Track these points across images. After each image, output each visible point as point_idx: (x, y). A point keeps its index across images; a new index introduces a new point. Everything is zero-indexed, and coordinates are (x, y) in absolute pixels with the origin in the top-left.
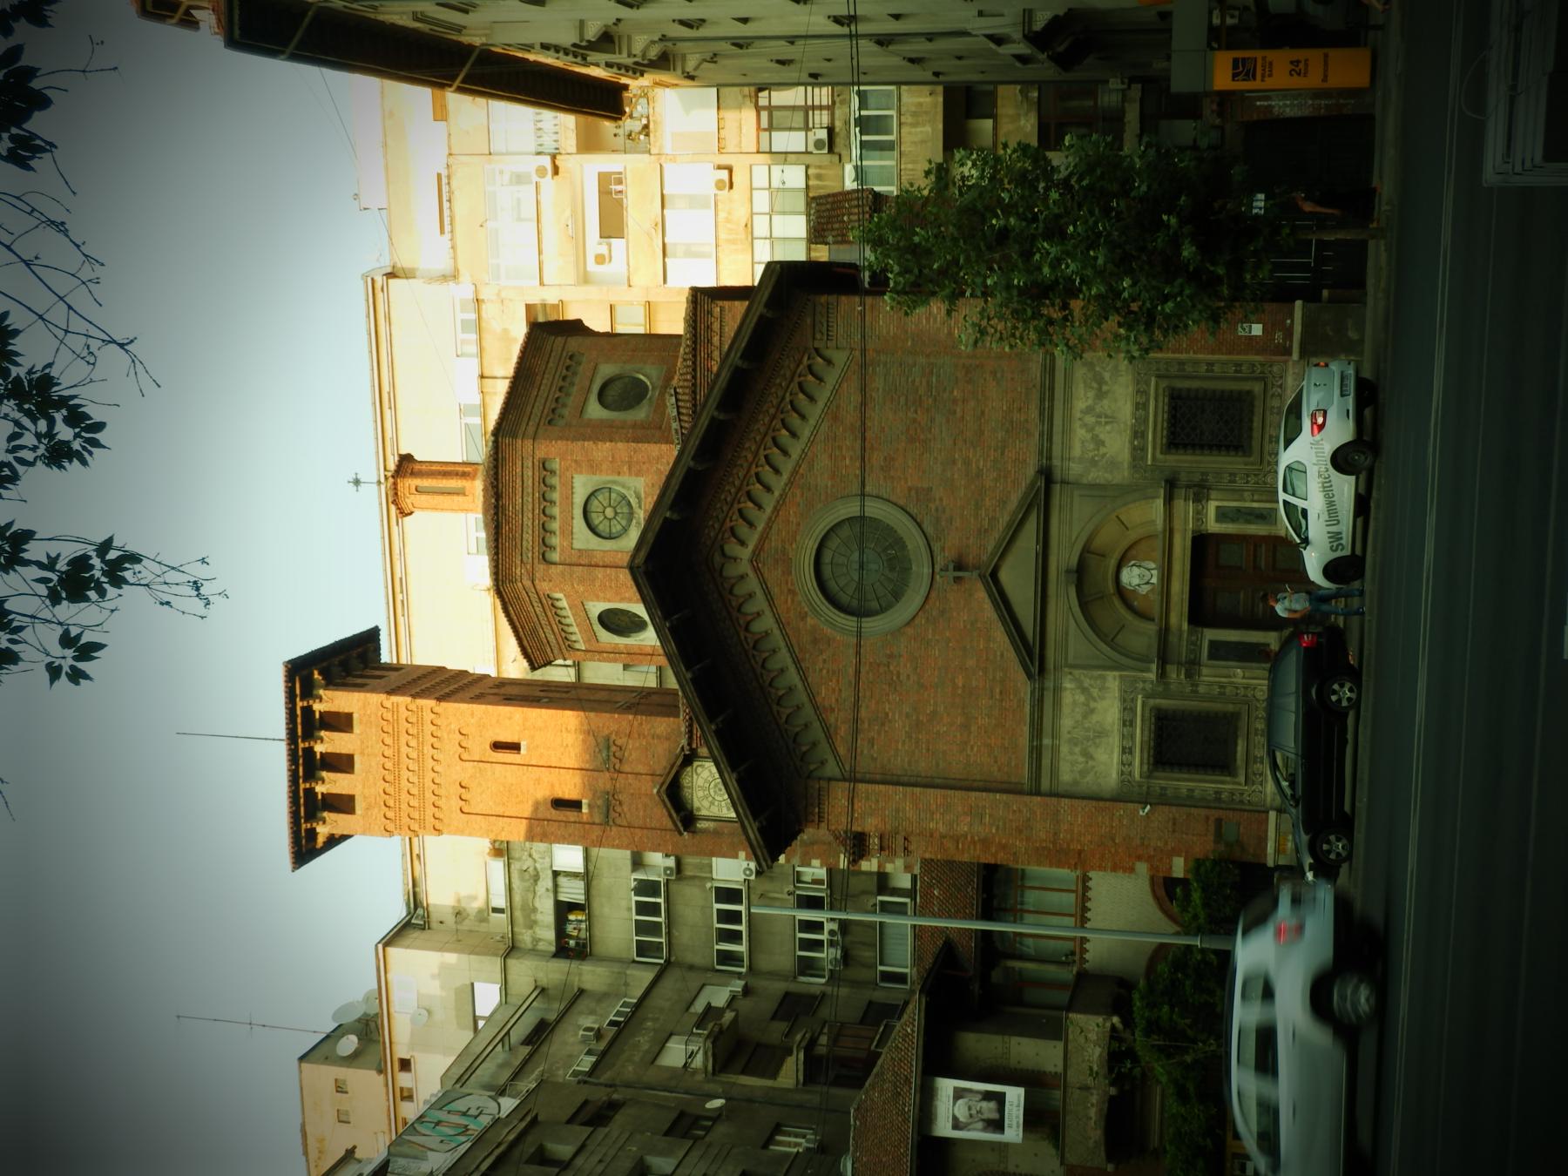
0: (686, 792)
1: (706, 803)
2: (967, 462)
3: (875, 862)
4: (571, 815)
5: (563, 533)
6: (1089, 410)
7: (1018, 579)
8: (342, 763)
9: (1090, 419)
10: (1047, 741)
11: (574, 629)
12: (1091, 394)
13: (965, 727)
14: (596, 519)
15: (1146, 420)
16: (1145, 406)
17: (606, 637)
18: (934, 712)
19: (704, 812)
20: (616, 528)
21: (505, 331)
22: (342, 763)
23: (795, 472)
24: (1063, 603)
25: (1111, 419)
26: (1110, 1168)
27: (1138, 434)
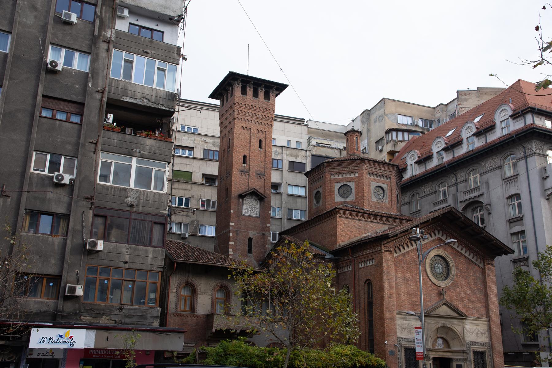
0: (250, 197)
1: (247, 202)
2: (465, 297)
3: (232, 253)
4: (242, 160)
5: (374, 179)
6: (479, 330)
7: (444, 310)
8: (256, 95)
9: (477, 330)
10: (407, 317)
11: (340, 177)
12: (482, 331)
13: (408, 294)
14: (380, 189)
15: (478, 345)
16: (481, 345)
17: (339, 185)
18: (411, 285)
19: (244, 202)
20: (341, 190)
21: (299, 156)
22: (256, 95)
23: (458, 252)
24: (439, 323)
25: (477, 336)
26: (214, 330)
27: (475, 343)
